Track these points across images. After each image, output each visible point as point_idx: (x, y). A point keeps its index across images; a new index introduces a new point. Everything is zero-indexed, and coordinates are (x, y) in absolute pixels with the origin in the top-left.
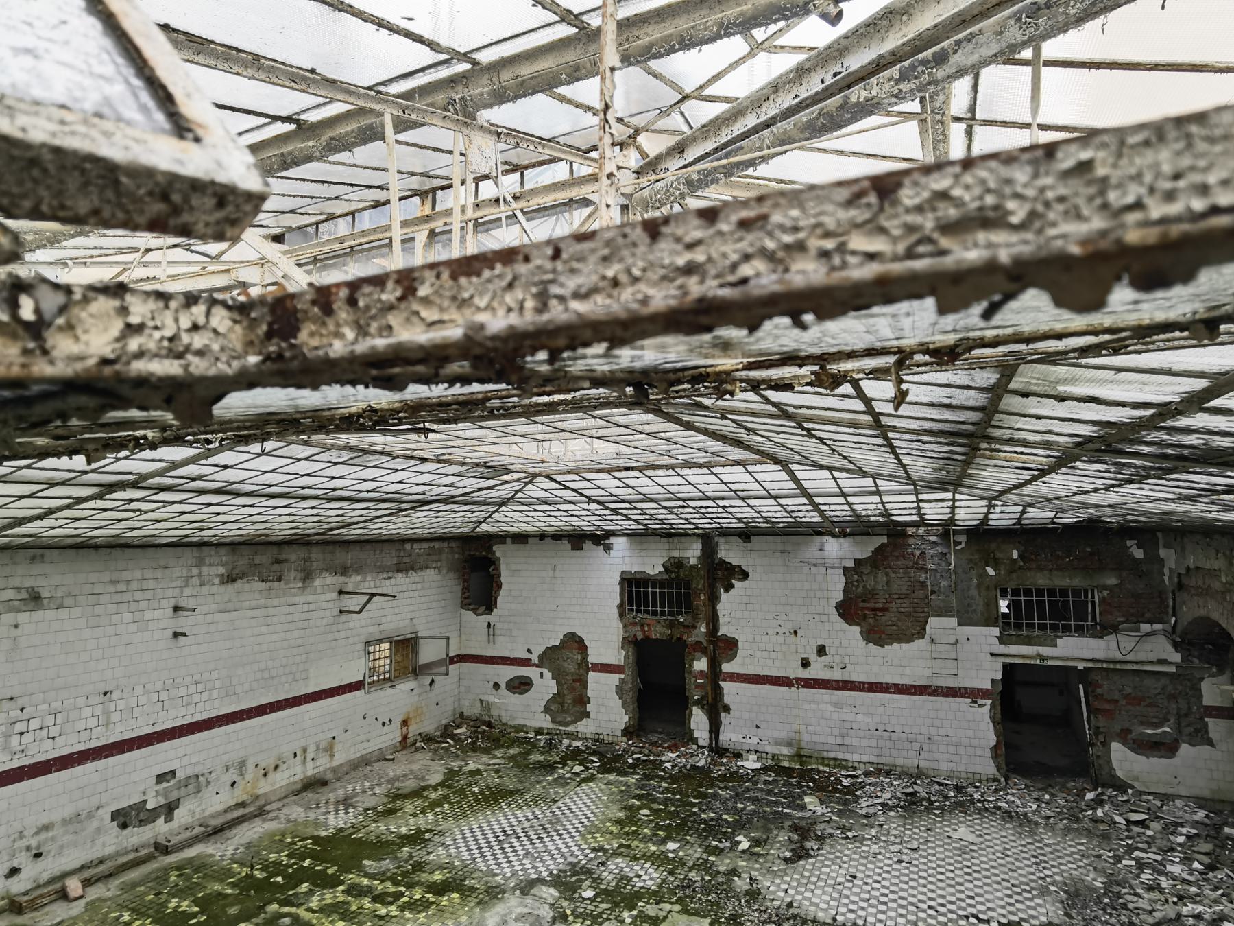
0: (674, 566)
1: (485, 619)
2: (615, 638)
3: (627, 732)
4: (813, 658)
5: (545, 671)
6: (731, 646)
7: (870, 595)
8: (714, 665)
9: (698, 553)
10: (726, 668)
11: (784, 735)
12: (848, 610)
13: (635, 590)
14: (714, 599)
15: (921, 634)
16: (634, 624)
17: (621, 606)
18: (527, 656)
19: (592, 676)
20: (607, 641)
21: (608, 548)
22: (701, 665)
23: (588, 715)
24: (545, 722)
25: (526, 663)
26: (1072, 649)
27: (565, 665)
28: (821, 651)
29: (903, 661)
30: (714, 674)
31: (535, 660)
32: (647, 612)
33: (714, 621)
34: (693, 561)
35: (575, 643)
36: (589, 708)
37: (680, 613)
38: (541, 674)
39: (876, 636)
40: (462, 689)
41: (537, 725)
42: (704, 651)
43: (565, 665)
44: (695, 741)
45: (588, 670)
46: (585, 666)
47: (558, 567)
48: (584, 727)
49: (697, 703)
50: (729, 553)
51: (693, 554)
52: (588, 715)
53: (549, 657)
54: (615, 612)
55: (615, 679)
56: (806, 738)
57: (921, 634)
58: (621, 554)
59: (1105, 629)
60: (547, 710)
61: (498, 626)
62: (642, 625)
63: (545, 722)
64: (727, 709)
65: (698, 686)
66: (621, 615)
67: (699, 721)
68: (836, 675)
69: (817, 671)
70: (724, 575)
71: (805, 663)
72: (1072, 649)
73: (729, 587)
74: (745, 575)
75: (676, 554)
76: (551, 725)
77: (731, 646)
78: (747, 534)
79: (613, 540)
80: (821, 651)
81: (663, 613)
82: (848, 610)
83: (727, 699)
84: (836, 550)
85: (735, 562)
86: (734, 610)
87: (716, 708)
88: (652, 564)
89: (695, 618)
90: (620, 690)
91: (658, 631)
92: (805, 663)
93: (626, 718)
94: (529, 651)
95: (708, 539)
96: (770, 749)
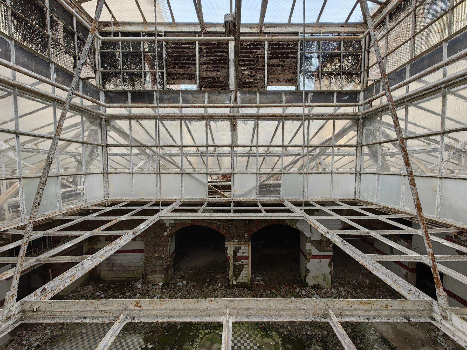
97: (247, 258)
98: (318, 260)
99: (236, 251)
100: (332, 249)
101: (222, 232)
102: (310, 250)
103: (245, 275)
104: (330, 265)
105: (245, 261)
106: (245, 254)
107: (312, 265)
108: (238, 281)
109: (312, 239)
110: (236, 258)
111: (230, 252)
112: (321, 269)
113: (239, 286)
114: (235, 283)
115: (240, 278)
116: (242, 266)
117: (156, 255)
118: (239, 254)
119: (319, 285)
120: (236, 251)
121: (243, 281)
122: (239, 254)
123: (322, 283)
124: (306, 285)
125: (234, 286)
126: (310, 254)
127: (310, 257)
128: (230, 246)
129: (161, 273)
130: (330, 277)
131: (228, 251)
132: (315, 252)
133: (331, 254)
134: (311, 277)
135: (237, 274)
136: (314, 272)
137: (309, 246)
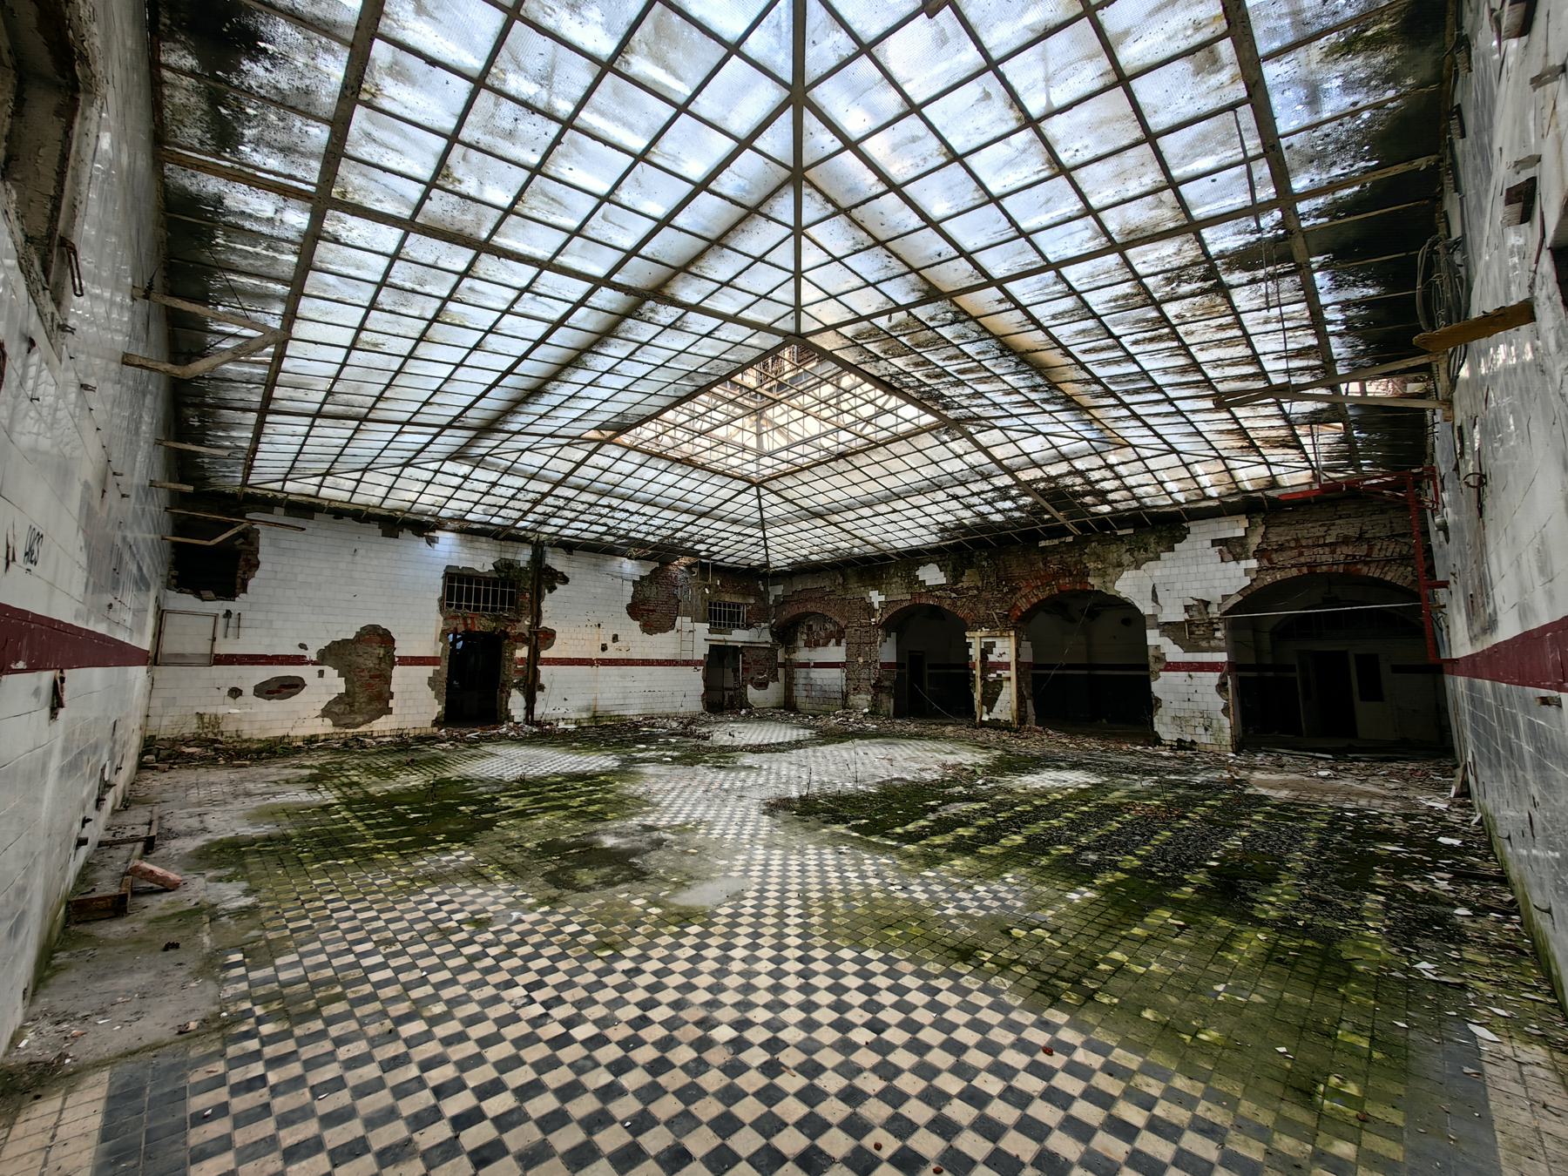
0: (504, 567)
1: (219, 607)
2: (433, 630)
3: (436, 723)
4: (610, 644)
5: (328, 670)
6: (550, 636)
7: (646, 601)
8: (535, 653)
9: (528, 558)
10: (544, 654)
11: (585, 703)
12: (634, 610)
13: (457, 584)
14: (540, 597)
15: (672, 627)
16: (456, 617)
17: (441, 600)
18: (301, 652)
19: (398, 671)
20: (421, 631)
21: (431, 541)
22: (522, 652)
23: (389, 711)
24: (324, 727)
25: (298, 660)
26: (739, 636)
27: (361, 660)
28: (615, 638)
29: (662, 645)
30: (534, 660)
31: (312, 655)
32: (468, 607)
33: (537, 615)
34: (523, 564)
35: (377, 637)
36: (392, 703)
37: (502, 609)
38: (321, 673)
39: (649, 628)
40: (156, 703)
41: (308, 732)
42: (526, 641)
43: (361, 660)
44: (510, 718)
45: (394, 664)
46: (390, 660)
47: (360, 552)
48: (383, 726)
49: (516, 686)
50: (556, 561)
51: (524, 556)
52: (389, 711)
53: (335, 654)
54: (435, 606)
55: (428, 671)
56: (600, 703)
57: (672, 627)
58: (447, 548)
59: (748, 626)
60: (326, 713)
61: (246, 616)
62: (465, 619)
63: (324, 727)
64: (542, 688)
65: (518, 671)
66: (441, 609)
67: (516, 704)
68: (624, 655)
69: (611, 653)
70: (550, 579)
71: (604, 648)
72: (739, 636)
73: (552, 589)
74: (566, 580)
75: (509, 556)
76: (331, 730)
77: (550, 636)
78: (569, 547)
79: (439, 534)
80: (615, 638)
81: (485, 609)
82: (634, 610)
83: (543, 680)
84: (630, 568)
85: (559, 569)
86: (554, 609)
87: (531, 688)
88: (482, 559)
89: (519, 612)
90: (432, 682)
91: (483, 624)
92: (604, 648)
93: (439, 708)
94: (303, 646)
95: (538, 548)
96: (574, 716)
97: (1007, 666)
98: (1185, 674)
99: (987, 650)
100: (1223, 644)
101: (961, 613)
102: (1157, 647)
103: (1006, 704)
104: (1221, 688)
105: (1005, 674)
106: (1005, 659)
107: (1164, 685)
108: (993, 716)
109: (1163, 619)
110: (987, 667)
111: (975, 652)
112: (1197, 697)
113: (995, 725)
114: (985, 718)
115: (995, 709)
116: (998, 684)
117: (861, 660)
118: (992, 658)
119: (1193, 742)
120: (987, 650)
121: (1002, 717)
122: (992, 658)
123: (1204, 738)
124: (1157, 741)
125: (983, 724)
126: (1160, 658)
127: (1162, 666)
128: (976, 641)
129: (867, 693)
130: (1226, 722)
131: (971, 652)
132: (1174, 653)
133: (1222, 657)
134: (1167, 719)
135: (990, 701)
136: (1176, 705)
137: (1153, 637)
